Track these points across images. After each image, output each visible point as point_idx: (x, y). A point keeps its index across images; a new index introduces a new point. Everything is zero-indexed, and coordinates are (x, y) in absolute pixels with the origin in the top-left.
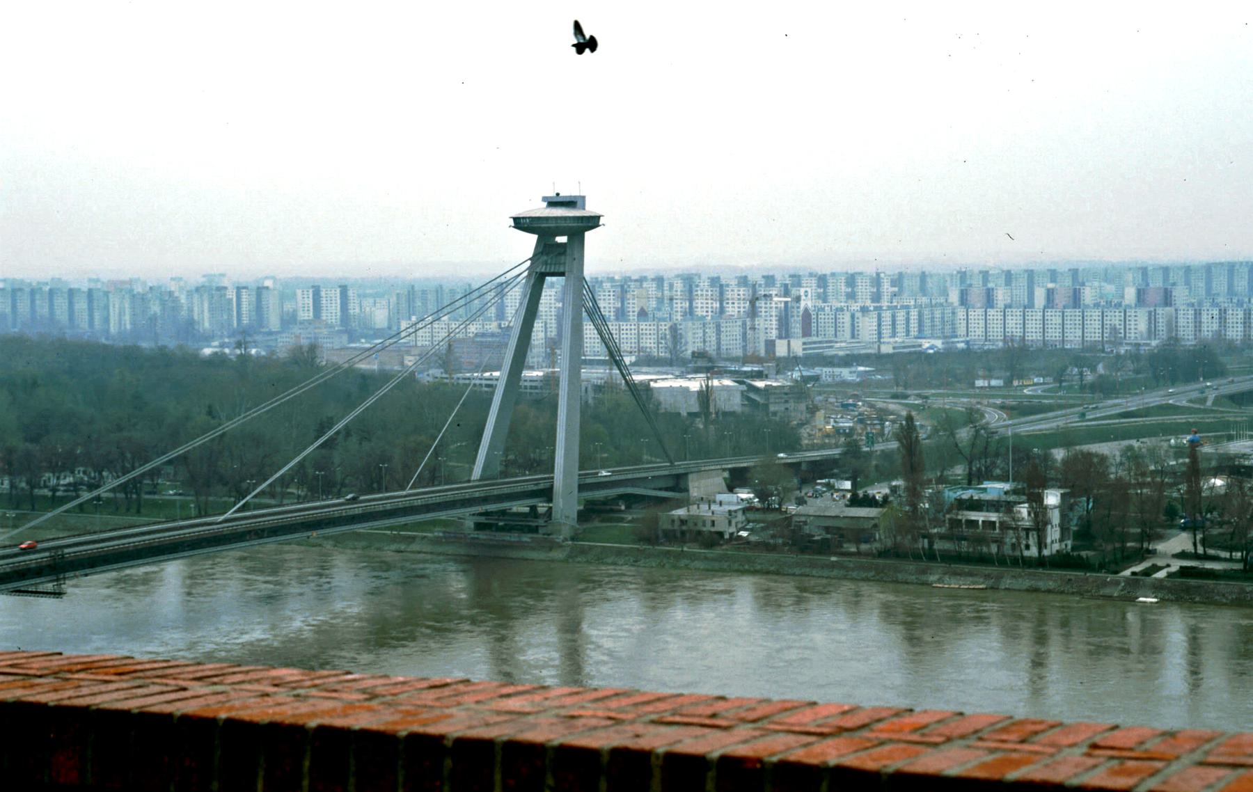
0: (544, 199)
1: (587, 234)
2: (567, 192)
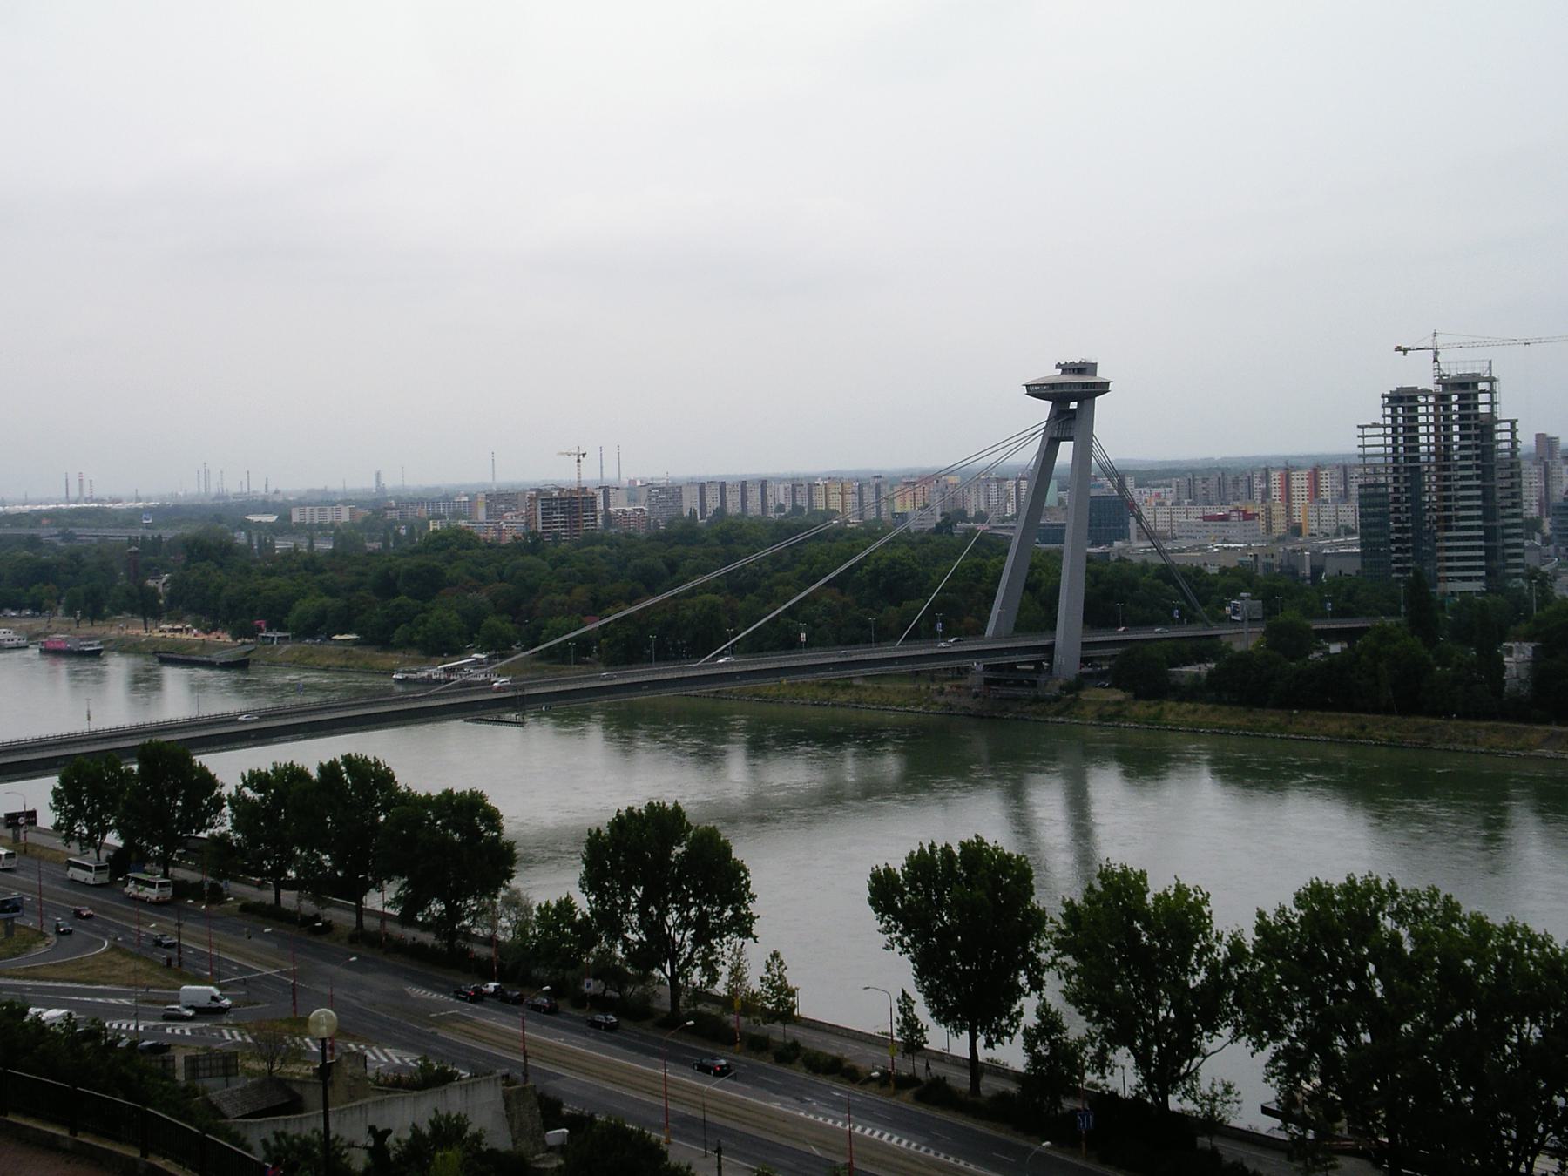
0: (1058, 366)
1: (1097, 399)
2: (1077, 358)
